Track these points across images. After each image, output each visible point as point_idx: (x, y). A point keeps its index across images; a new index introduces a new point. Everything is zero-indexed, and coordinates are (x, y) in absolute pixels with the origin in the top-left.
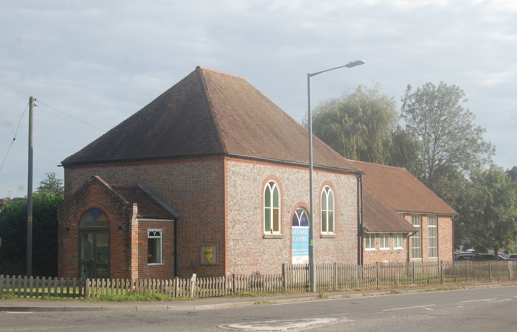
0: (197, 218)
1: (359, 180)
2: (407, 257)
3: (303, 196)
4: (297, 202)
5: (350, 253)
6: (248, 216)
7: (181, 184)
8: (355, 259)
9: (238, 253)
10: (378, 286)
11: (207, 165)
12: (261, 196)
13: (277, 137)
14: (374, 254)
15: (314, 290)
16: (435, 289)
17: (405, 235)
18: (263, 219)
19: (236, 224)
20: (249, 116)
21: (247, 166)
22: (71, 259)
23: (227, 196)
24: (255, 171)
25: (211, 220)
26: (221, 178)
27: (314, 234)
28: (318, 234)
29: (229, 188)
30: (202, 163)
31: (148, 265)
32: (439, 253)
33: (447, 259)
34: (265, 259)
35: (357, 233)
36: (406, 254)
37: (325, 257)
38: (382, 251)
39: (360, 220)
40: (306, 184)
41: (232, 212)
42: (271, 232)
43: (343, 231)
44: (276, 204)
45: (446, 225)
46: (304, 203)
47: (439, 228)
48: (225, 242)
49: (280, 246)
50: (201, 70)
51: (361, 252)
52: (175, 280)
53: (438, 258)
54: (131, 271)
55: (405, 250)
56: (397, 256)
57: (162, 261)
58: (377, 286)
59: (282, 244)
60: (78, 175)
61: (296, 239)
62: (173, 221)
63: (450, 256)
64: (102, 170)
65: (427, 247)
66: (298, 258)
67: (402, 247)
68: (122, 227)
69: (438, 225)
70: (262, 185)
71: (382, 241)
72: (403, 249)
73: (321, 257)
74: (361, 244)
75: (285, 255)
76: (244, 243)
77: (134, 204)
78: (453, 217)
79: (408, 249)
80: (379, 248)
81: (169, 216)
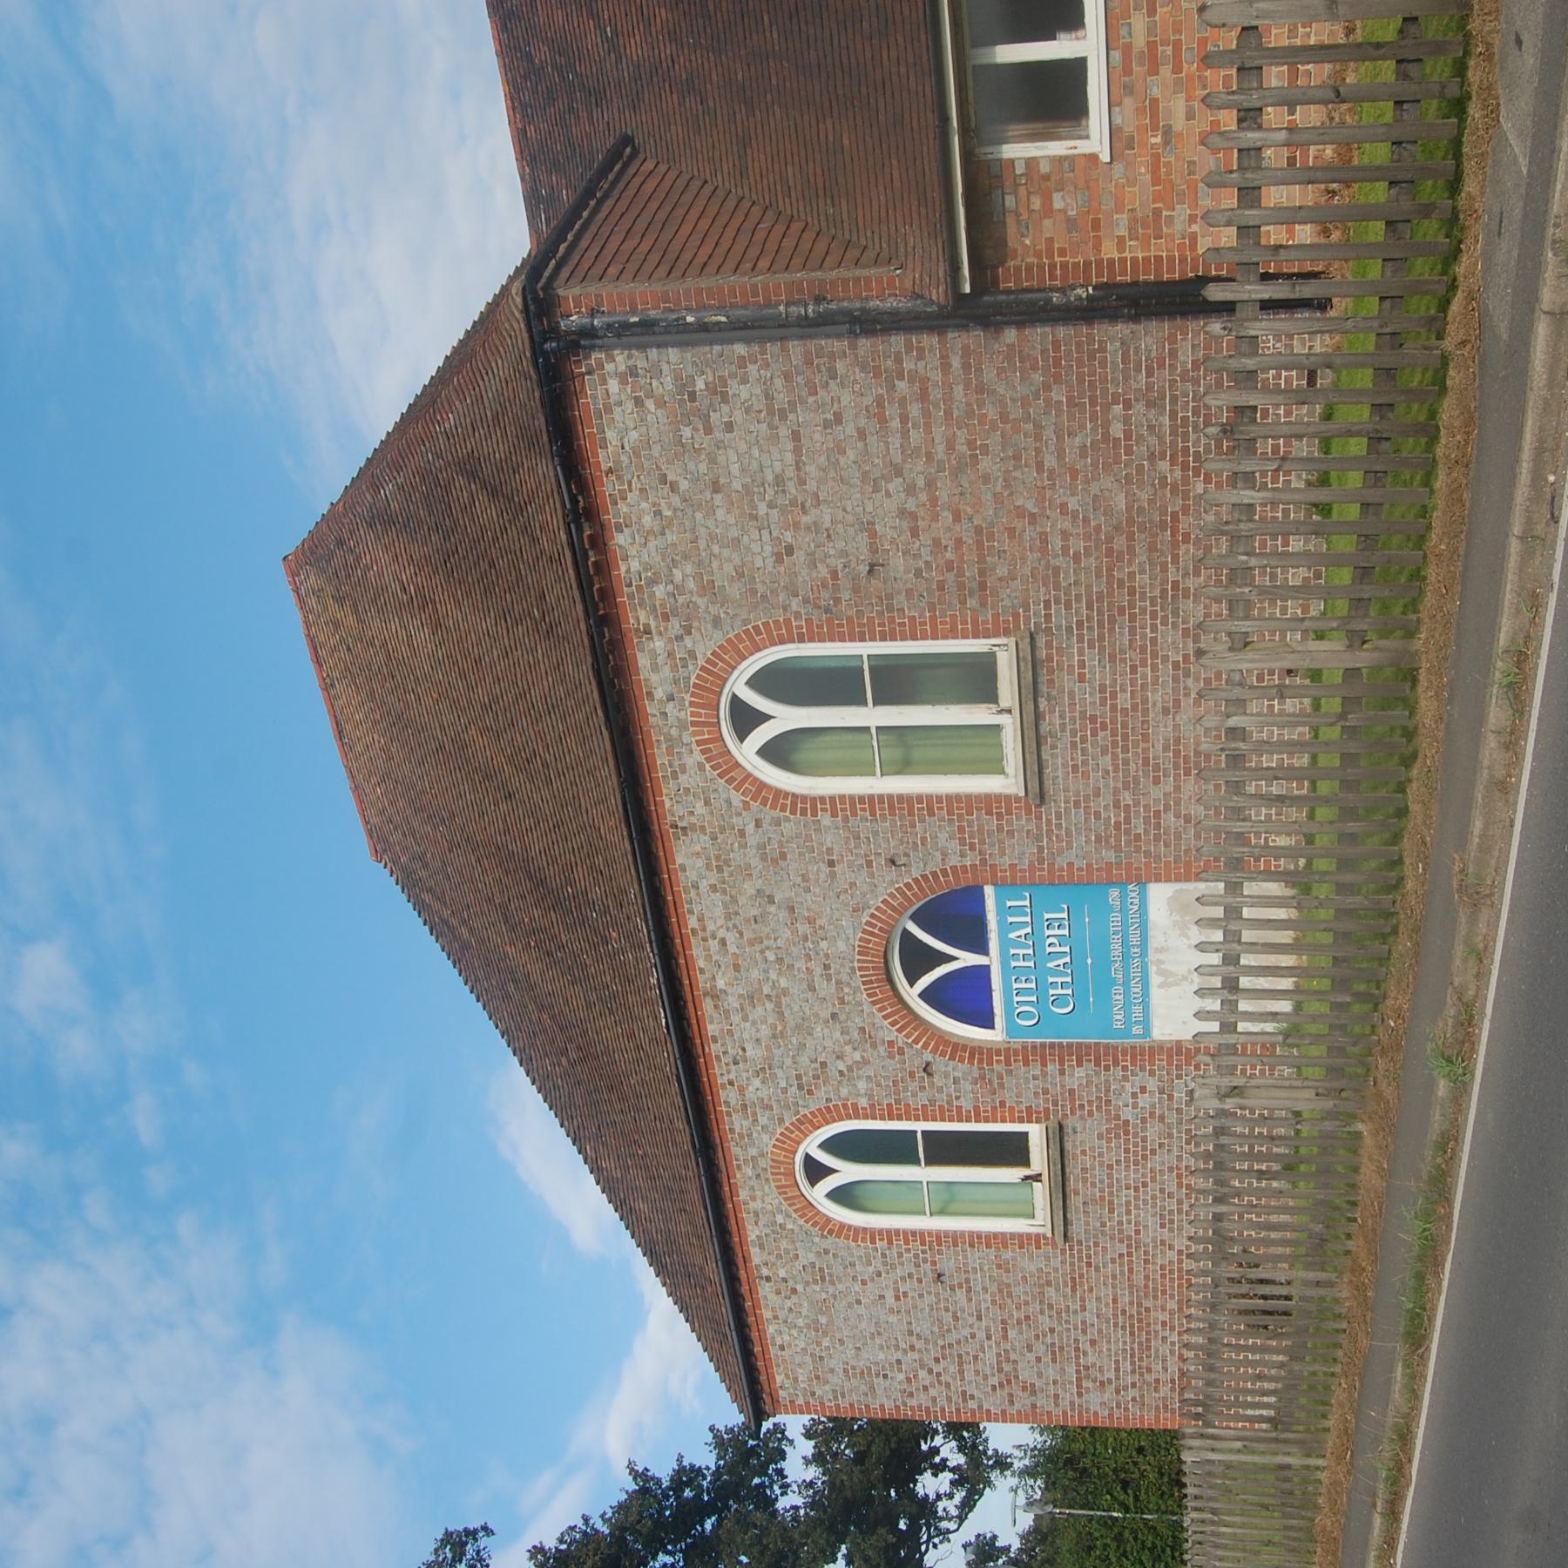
5: (1128, 436)
9: (1133, 1372)
19: (1017, 1377)
23: (912, 1408)
28: (1022, 823)
34: (1163, 1226)
41: (972, 1390)
59: (1089, 1121)
66: (1160, 972)
70: (831, 1240)
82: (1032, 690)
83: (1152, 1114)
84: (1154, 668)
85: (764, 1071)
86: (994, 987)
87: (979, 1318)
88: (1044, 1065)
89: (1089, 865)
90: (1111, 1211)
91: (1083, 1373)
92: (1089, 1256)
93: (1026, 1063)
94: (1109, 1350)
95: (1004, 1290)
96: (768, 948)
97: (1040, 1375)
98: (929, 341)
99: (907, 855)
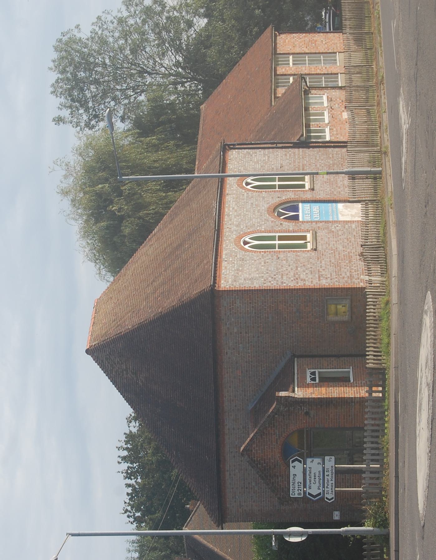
0: (293, 327)
1: (233, 147)
2: (337, 89)
3: (259, 209)
4: (268, 216)
5: (333, 157)
6: (289, 266)
7: (248, 350)
8: (341, 151)
10: (376, 105)
11: (225, 314)
12: (262, 253)
13: (180, 245)
14: (335, 129)
15: (380, 170)
16: (378, 37)
17: (307, 93)
18: (291, 251)
19: (299, 278)
20: (154, 281)
21: (226, 268)
22: (347, 484)
23: (265, 286)
24: (230, 260)
25: (295, 307)
26: (242, 294)
27: (309, 196)
29: (255, 285)
30: (223, 320)
31: (352, 381)
32: (330, 51)
33: (340, 40)
34: (343, 247)
35: (305, 149)
36: (333, 91)
37: (339, 185)
38: (330, 120)
39: (287, 145)
40: (243, 206)
42: (308, 244)
43: (303, 165)
44: (273, 238)
45: (289, 42)
46: (269, 208)
47: (292, 52)
48: (322, 288)
49: (326, 233)
50: (91, 347)
51: (331, 144)
52: (367, 293)
53: (337, 53)
54: (360, 398)
55: (328, 92)
56: (336, 101)
57: (347, 369)
58: (375, 106)
59: (323, 231)
60: (235, 501)
62: (296, 359)
63: (334, 36)
64: (230, 465)
65: (322, 68)
66: (341, 214)
67: (324, 96)
68: (305, 411)
69: (289, 54)
71: (315, 120)
72: (326, 94)
73: (339, 189)
74: (321, 144)
75: (337, 228)
76: (324, 270)
77: (276, 395)
78: (276, 32)
79: (326, 88)
80: (326, 124)
81: (290, 364)
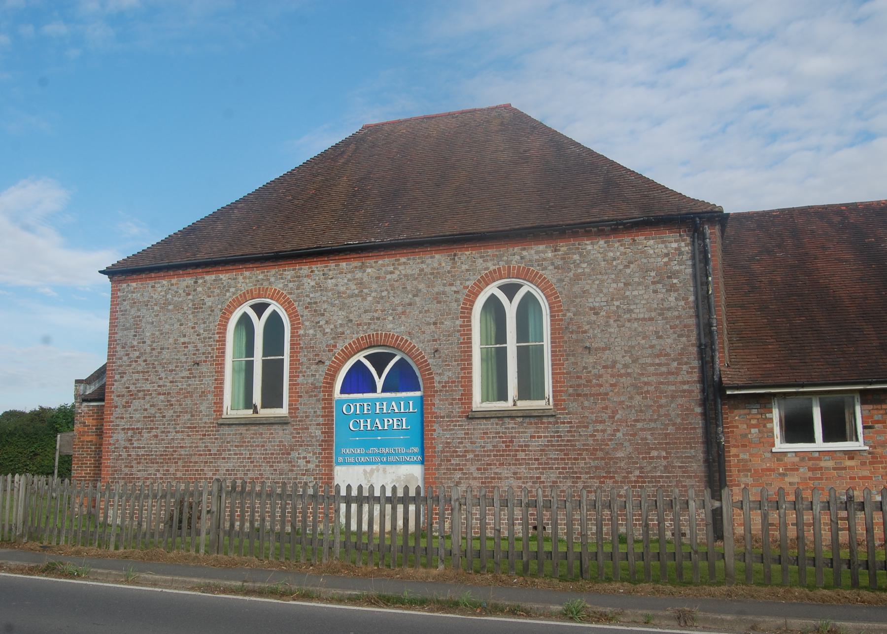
9: (138, 455)
14: (849, 463)
19: (135, 399)
27: (440, 406)
28: (457, 409)
34: (228, 470)
59: (291, 437)
61: (362, 424)
66: (372, 471)
70: (220, 314)
82: (528, 415)
83: (294, 466)
84: (537, 469)
85: (318, 287)
86: (365, 394)
87: (171, 382)
88: (323, 416)
89: (434, 439)
90: (236, 446)
91: (138, 431)
92: (209, 435)
93: (323, 408)
94: (152, 444)
95: (190, 394)
96: (389, 293)
97: (136, 410)
98: (696, 377)
99: (440, 357)
